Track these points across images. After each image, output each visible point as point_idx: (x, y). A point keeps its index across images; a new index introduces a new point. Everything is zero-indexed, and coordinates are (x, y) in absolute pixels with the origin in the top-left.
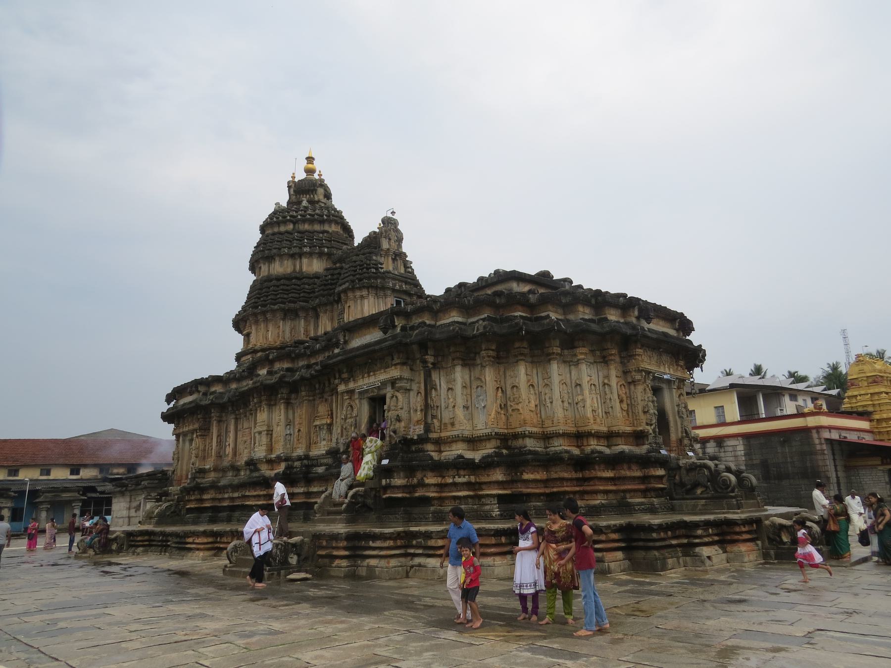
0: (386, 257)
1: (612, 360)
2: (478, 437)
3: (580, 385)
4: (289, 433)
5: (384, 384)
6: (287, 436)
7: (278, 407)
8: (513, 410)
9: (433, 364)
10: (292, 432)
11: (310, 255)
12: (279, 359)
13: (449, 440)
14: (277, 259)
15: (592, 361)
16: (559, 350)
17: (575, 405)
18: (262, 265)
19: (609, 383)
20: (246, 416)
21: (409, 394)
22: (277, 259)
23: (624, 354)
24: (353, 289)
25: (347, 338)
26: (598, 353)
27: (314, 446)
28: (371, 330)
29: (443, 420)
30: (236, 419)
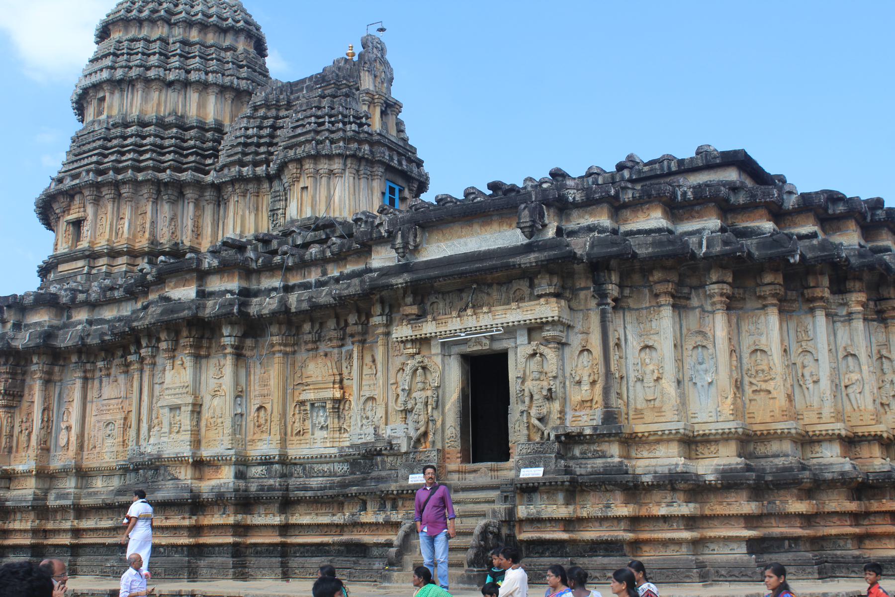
0: (372, 106)
2: (704, 435)
3: (854, 355)
4: (239, 411)
5: (510, 331)
6: (236, 418)
7: (213, 361)
8: (754, 391)
9: (615, 300)
11: (204, 86)
12: (224, 269)
13: (651, 438)
14: (139, 86)
16: (827, 294)
17: (843, 388)
18: (107, 95)
20: (108, 375)
22: (139, 86)
24: (316, 157)
25: (418, 240)
27: (294, 438)
28: (476, 227)
29: (632, 401)
30: (85, 380)
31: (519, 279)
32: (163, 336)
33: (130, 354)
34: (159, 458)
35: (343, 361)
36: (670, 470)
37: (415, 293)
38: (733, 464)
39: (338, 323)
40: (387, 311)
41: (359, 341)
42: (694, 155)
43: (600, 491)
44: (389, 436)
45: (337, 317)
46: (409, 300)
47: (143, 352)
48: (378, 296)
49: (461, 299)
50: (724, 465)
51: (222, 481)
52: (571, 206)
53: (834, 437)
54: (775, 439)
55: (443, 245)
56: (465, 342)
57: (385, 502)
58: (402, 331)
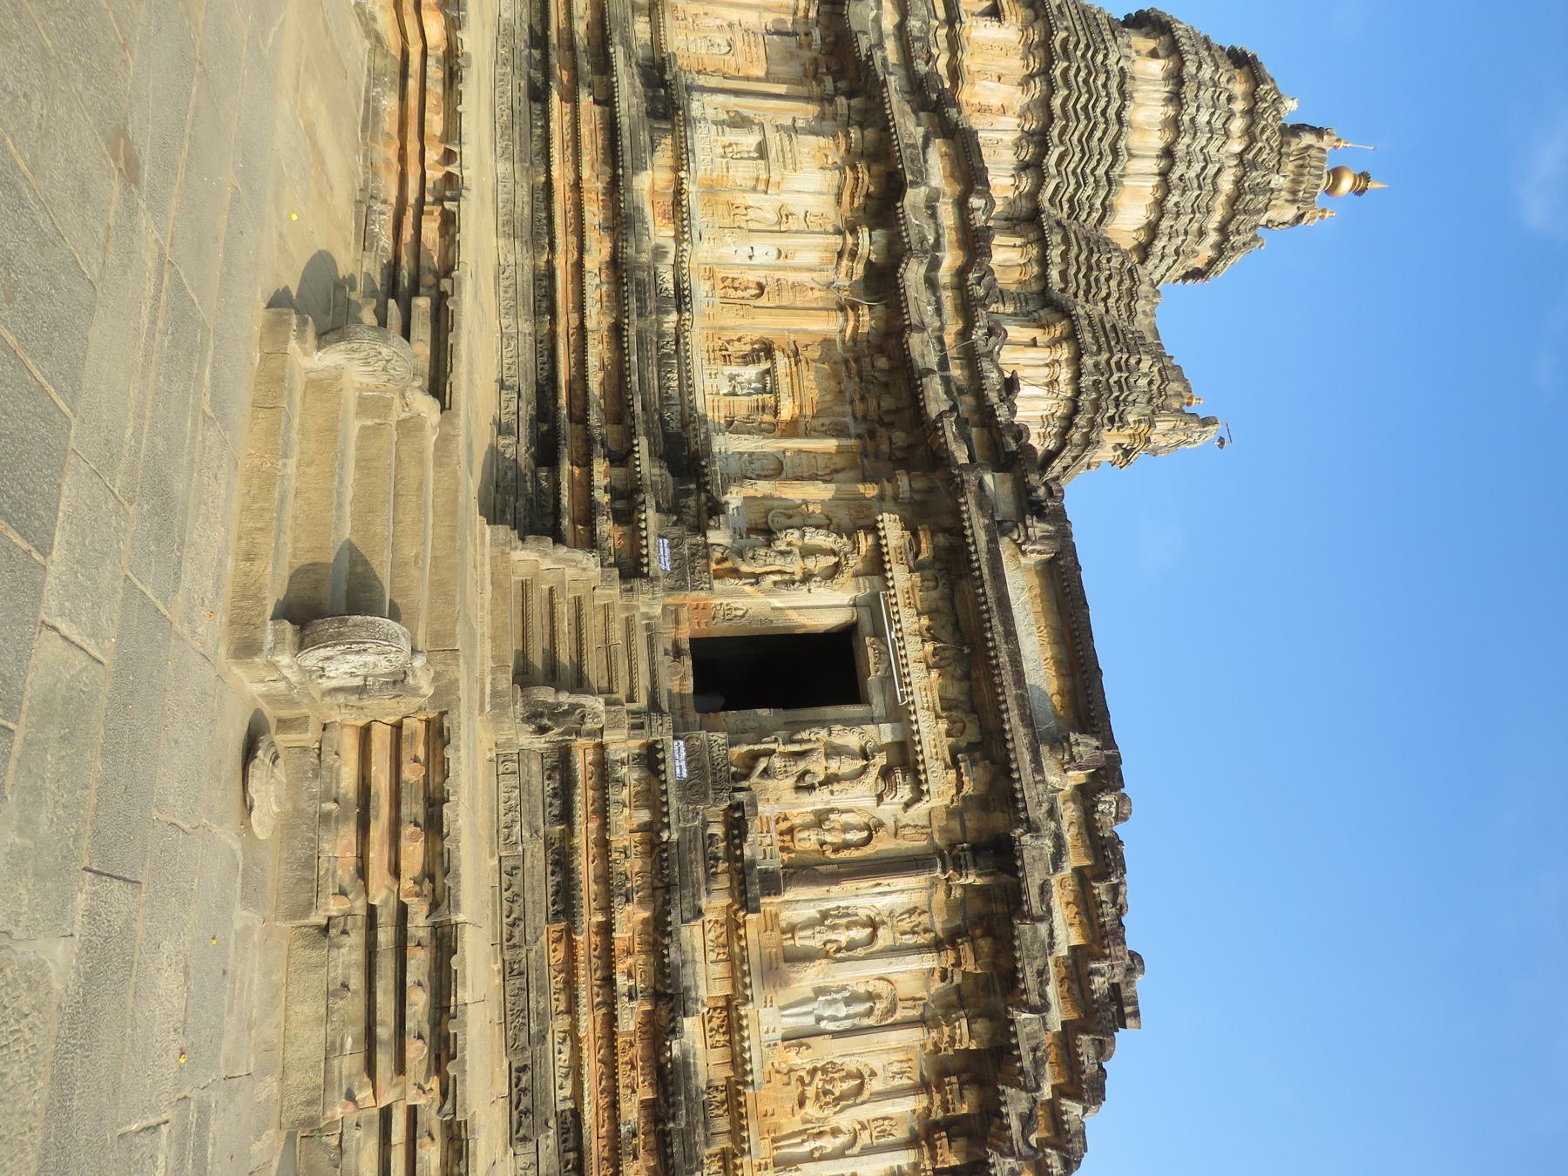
2: (741, 1028)
5: (899, 714)
20: (800, 46)
31: (981, 727)
32: (870, 133)
33: (835, 81)
34: (688, 121)
35: (832, 419)
36: (688, 989)
37: (951, 550)
38: (697, 1079)
39: (888, 412)
40: (916, 497)
41: (865, 448)
42: (1130, 947)
43: (654, 877)
44: (727, 503)
45: (898, 411)
46: (941, 539)
47: (841, 101)
48: (939, 484)
49: (943, 627)
51: (651, 225)
52: (1088, 803)
54: (732, 1122)
55: (1025, 596)
56: (879, 633)
57: (623, 498)
58: (893, 531)
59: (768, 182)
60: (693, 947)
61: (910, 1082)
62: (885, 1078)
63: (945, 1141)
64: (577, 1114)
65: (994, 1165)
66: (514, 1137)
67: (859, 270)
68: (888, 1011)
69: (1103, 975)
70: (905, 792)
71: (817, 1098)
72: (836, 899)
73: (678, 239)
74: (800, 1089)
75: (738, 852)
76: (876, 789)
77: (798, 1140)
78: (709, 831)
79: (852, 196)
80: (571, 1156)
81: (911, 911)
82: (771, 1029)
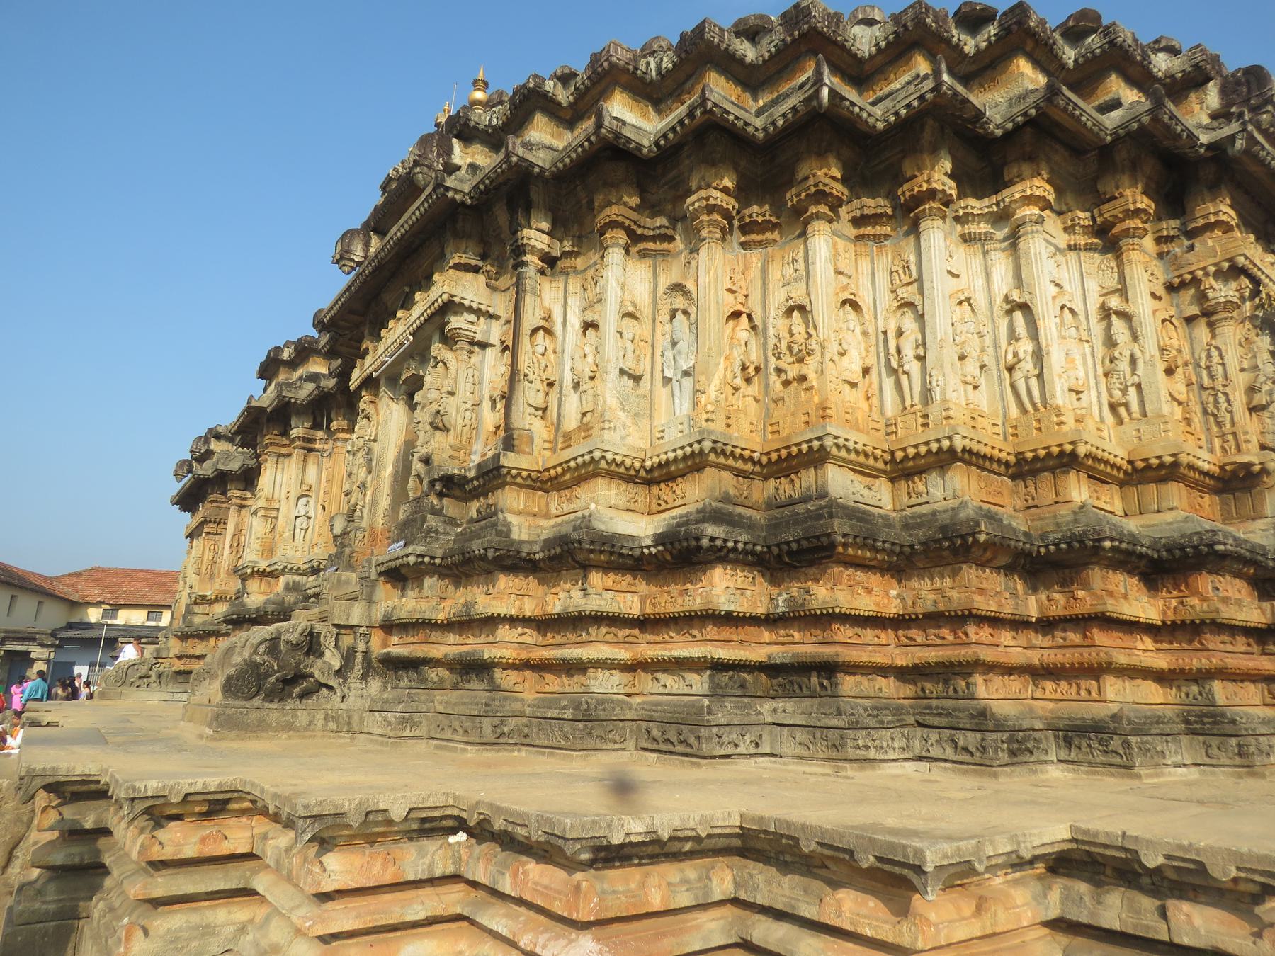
1: (1126, 233)
2: (660, 464)
3: (1025, 307)
4: (302, 513)
10: (311, 514)
15: (1063, 245)
16: (951, 187)
19: (1125, 308)
21: (483, 361)
23: (1170, 226)
26: (1083, 217)
50: (681, 517)
53: (943, 457)
59: (266, 509)
60: (554, 526)
61: (802, 248)
62: (796, 280)
63: (906, 187)
64: (719, 666)
65: (896, 113)
66: (695, 751)
67: (320, 434)
68: (685, 293)
69: (661, 59)
70: (456, 322)
71: (801, 361)
72: (563, 372)
73: (283, 572)
74: (795, 384)
75: (476, 483)
76: (462, 349)
77: (904, 379)
78: (475, 516)
79: (284, 446)
80: (815, 680)
81: (585, 290)
82: (680, 427)
